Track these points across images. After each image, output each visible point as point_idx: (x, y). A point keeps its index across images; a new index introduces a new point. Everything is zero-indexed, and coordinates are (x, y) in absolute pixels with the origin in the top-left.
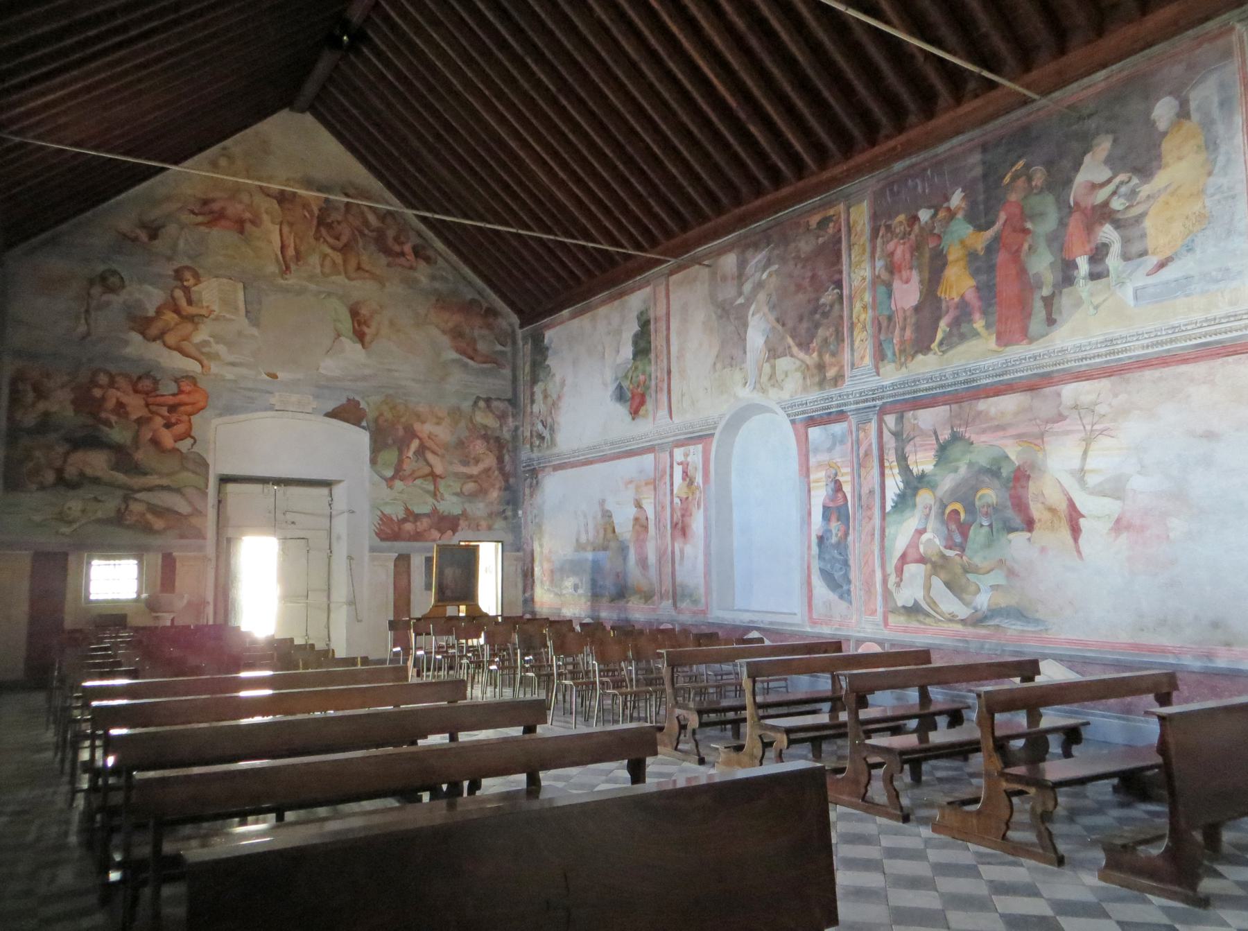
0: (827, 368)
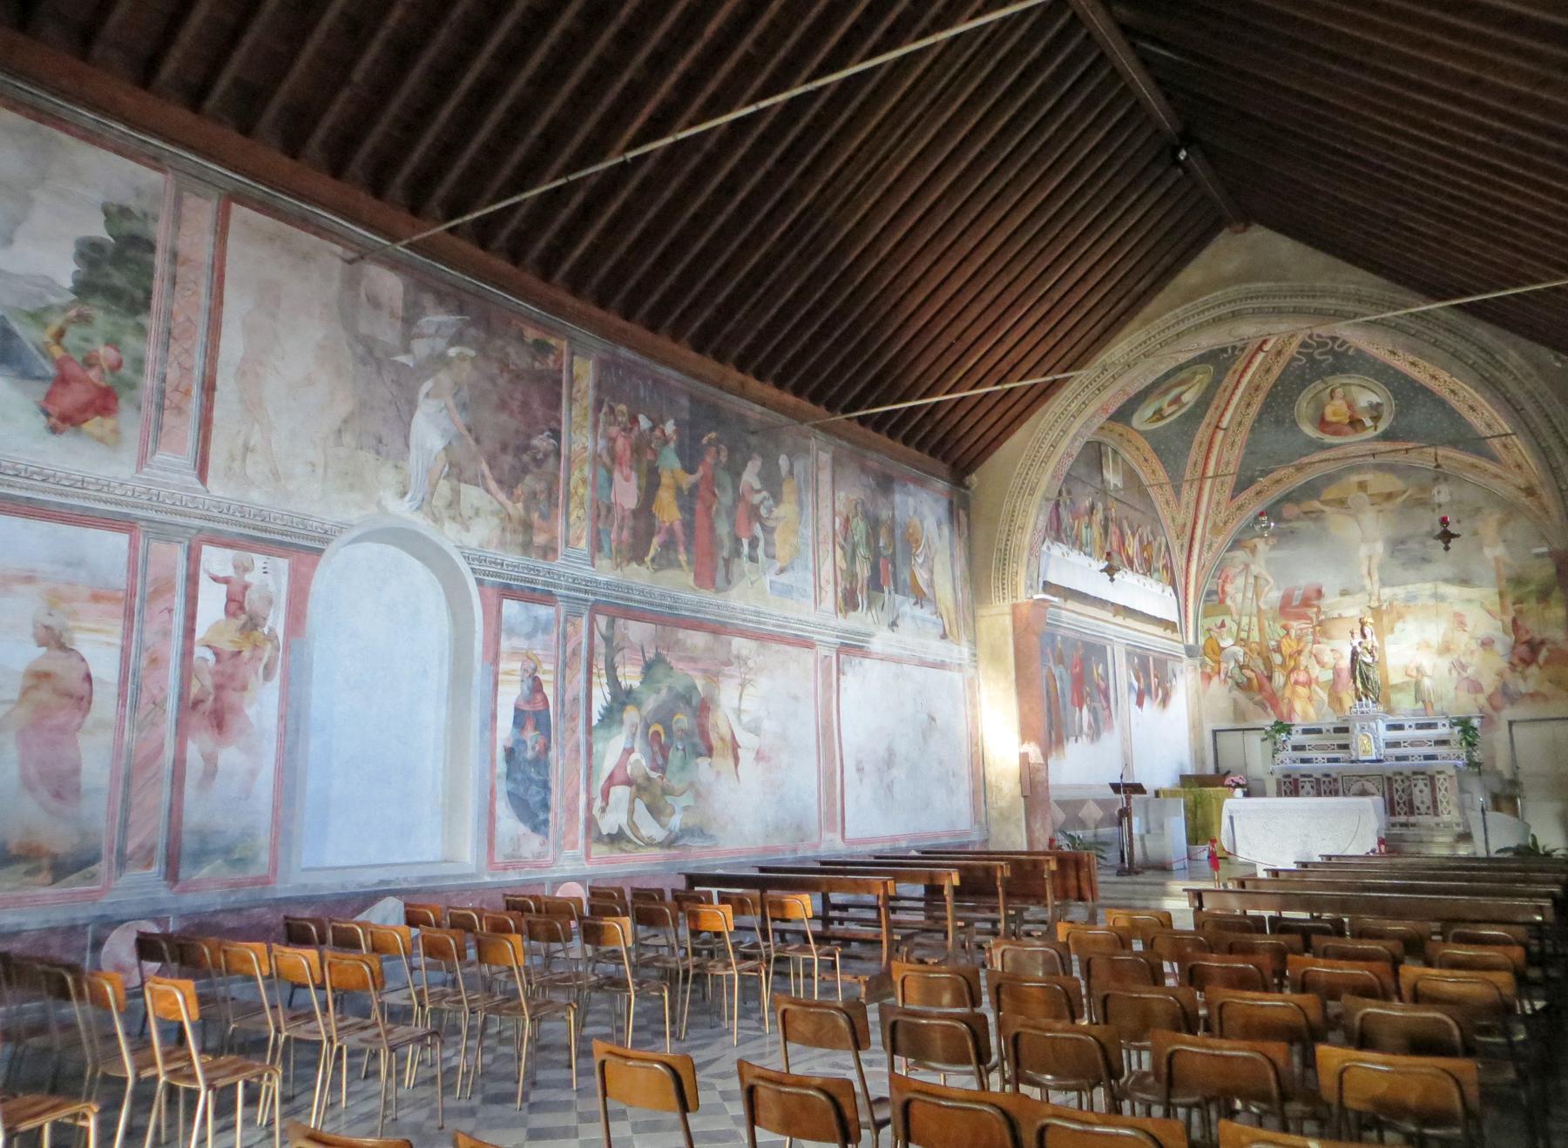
0: (535, 531)
